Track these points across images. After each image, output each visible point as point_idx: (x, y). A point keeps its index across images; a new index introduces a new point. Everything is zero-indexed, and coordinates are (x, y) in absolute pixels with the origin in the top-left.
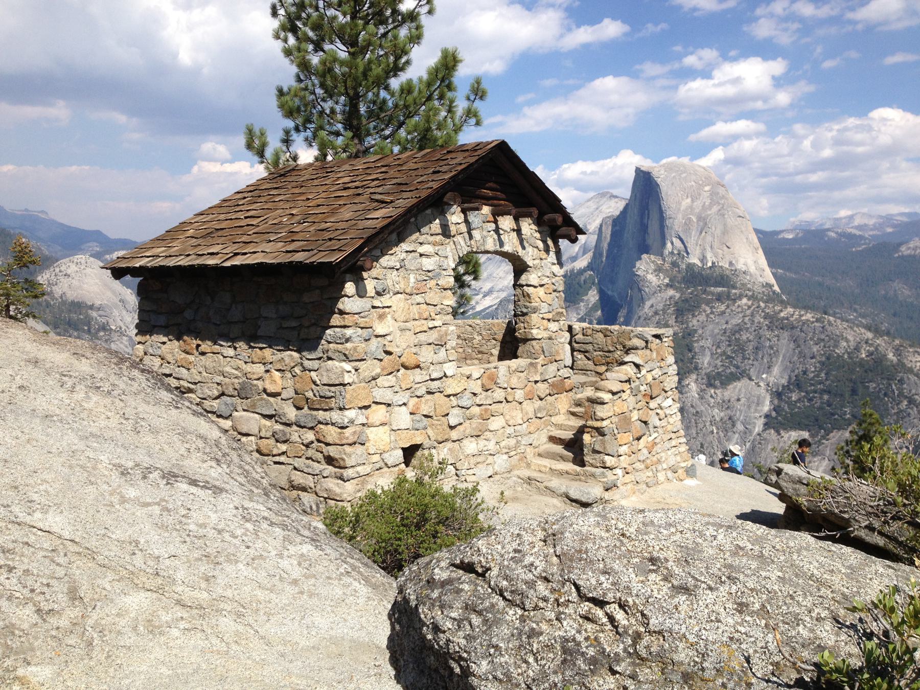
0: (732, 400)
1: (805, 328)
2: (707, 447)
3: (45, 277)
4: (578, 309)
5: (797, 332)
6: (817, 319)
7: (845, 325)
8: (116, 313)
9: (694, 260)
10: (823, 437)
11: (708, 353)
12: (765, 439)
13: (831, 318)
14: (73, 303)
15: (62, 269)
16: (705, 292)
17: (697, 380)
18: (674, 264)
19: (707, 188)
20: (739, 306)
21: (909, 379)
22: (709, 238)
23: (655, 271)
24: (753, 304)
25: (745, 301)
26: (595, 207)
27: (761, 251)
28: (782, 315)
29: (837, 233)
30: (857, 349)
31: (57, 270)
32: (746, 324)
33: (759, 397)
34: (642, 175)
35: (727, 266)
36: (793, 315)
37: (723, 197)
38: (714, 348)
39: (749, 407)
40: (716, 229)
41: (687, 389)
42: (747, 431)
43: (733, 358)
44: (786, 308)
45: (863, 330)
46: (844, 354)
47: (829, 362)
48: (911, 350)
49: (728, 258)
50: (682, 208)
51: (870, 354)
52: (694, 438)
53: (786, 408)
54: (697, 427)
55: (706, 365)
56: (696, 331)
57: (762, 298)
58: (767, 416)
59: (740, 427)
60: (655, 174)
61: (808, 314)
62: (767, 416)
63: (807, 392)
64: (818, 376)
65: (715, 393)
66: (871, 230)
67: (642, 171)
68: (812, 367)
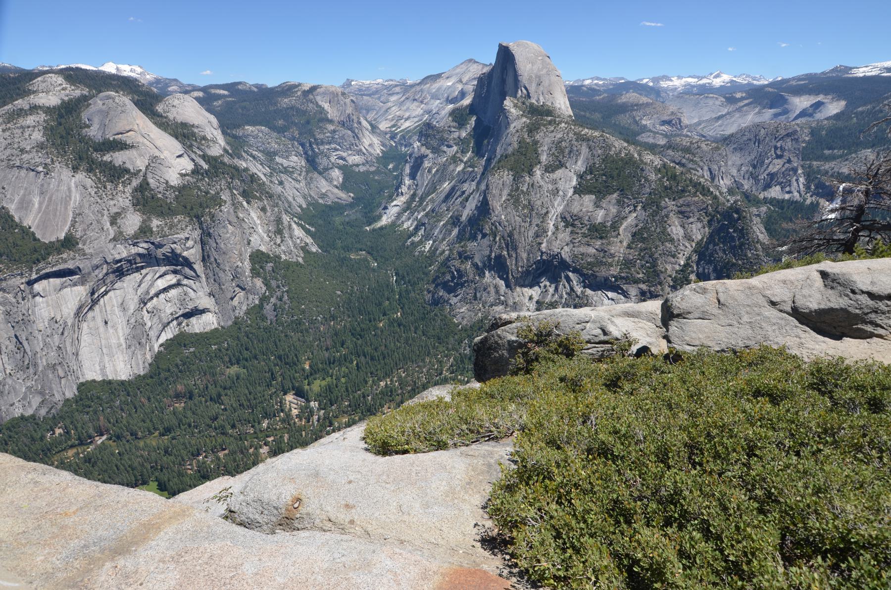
1: (595, 140)
3: (161, 108)
4: (466, 128)
5: (591, 143)
8: (208, 129)
9: (533, 101)
10: (604, 197)
11: (545, 154)
14: (182, 123)
15: (170, 102)
19: (540, 58)
22: (541, 88)
25: (563, 125)
28: (583, 133)
30: (620, 151)
31: (167, 103)
35: (550, 104)
40: (546, 83)
42: (565, 195)
47: (606, 159)
49: (551, 100)
51: (626, 155)
56: (539, 141)
58: (575, 188)
59: (561, 193)
60: (511, 48)
63: (595, 175)
64: (601, 166)
68: (597, 161)
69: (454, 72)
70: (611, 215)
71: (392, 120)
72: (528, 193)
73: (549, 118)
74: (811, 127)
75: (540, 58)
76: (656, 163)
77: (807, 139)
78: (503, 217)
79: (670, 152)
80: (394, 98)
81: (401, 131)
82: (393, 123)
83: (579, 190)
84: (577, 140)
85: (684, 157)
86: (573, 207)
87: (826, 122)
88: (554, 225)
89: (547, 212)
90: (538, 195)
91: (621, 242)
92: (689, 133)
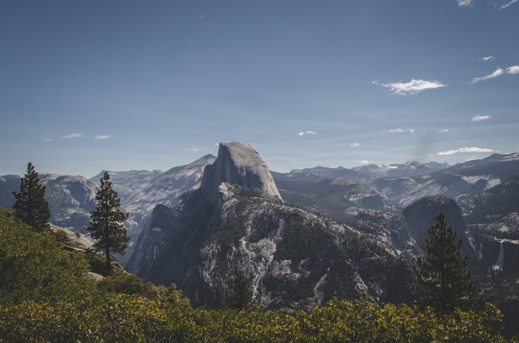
0: (260, 247)
2: (250, 270)
6: (294, 210)
7: (306, 212)
11: (250, 227)
12: (274, 264)
13: (300, 210)
16: (249, 199)
17: (245, 239)
18: (236, 187)
20: (263, 205)
21: (331, 234)
23: (228, 189)
24: (268, 204)
25: (265, 203)
26: (205, 161)
27: (273, 181)
28: (280, 208)
29: (309, 175)
32: (266, 213)
33: (271, 246)
34: (222, 147)
36: (285, 209)
37: (257, 158)
38: (253, 224)
39: (267, 250)
41: (241, 244)
42: (267, 261)
43: (260, 228)
44: (282, 205)
45: (313, 215)
46: (305, 225)
48: (332, 222)
50: (239, 162)
51: (316, 225)
52: (244, 266)
53: (282, 249)
54: (245, 261)
55: (249, 232)
56: (245, 217)
57: (273, 202)
59: (263, 259)
61: (291, 208)
62: (274, 254)
65: (253, 245)
66: (323, 174)
67: (222, 145)
69: (195, 165)
70: (306, 276)
71: (139, 204)
72: (235, 262)
73: (255, 198)
74: (474, 198)
75: (250, 154)
76: (341, 230)
77: (473, 207)
78: (211, 284)
79: (361, 222)
80: (144, 186)
81: (145, 213)
82: (139, 205)
83: (278, 256)
84: (276, 215)
85: (371, 226)
86: (273, 272)
87: (484, 194)
88: (257, 289)
89: (252, 277)
90: (244, 263)
91: (316, 301)
92: (389, 207)
